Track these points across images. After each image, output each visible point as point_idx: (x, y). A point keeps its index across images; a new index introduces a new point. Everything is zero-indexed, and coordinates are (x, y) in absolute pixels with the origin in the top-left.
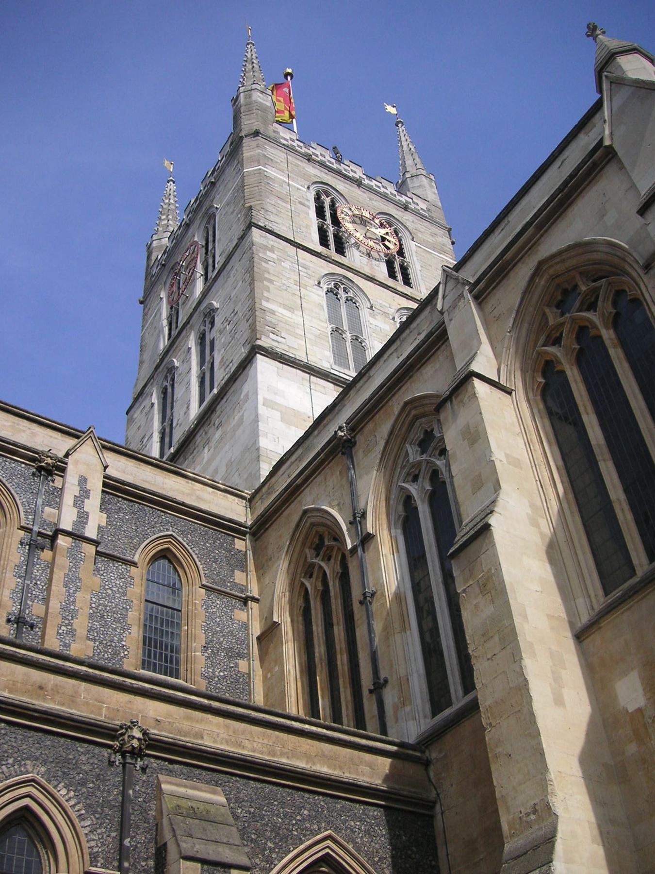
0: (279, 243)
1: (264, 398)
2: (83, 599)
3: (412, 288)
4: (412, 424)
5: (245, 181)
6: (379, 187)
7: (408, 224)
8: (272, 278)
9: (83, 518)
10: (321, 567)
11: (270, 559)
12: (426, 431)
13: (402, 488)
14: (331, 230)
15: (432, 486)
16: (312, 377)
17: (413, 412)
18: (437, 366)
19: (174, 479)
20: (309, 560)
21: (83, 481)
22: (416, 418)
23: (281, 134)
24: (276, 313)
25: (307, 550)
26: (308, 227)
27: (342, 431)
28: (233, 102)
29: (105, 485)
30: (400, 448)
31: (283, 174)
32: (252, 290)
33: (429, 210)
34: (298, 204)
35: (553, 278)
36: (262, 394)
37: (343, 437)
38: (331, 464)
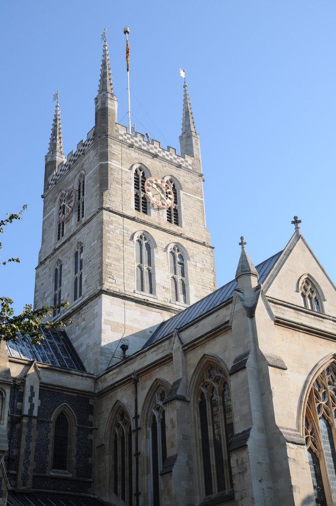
0: (115, 217)
2: (33, 445)
9: (32, 406)
17: (159, 383)
19: (67, 376)
21: (32, 388)
22: (160, 385)
23: (120, 132)
26: (130, 198)
29: (40, 386)
30: (154, 394)
32: (102, 251)
36: (104, 317)
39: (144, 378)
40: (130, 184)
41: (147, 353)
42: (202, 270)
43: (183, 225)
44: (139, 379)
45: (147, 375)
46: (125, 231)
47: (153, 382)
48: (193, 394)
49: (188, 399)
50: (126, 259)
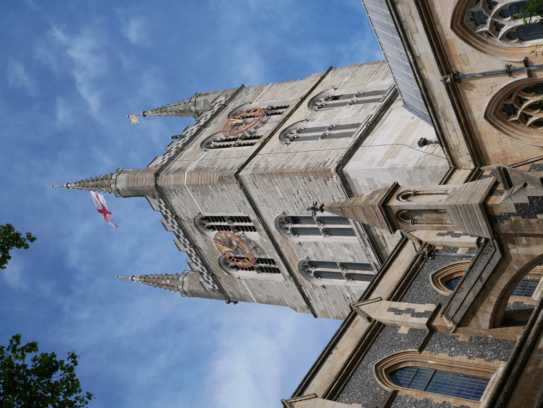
1: (377, 166)
3: (289, 106)
4: (464, 27)
5: (194, 183)
6: (206, 119)
7: (238, 105)
8: (281, 164)
10: (524, 109)
11: (504, 151)
12: (471, 20)
13: (501, 39)
17: (458, 24)
20: (516, 118)
22: (462, 23)
23: (158, 163)
24: (310, 162)
26: (238, 151)
27: (448, 78)
28: (118, 195)
31: (192, 163)
33: (226, 96)
34: (219, 156)
37: (451, 79)
38: (460, 92)
40: (221, 151)
42: (353, 76)
43: (293, 98)
46: (274, 152)
50: (308, 150)
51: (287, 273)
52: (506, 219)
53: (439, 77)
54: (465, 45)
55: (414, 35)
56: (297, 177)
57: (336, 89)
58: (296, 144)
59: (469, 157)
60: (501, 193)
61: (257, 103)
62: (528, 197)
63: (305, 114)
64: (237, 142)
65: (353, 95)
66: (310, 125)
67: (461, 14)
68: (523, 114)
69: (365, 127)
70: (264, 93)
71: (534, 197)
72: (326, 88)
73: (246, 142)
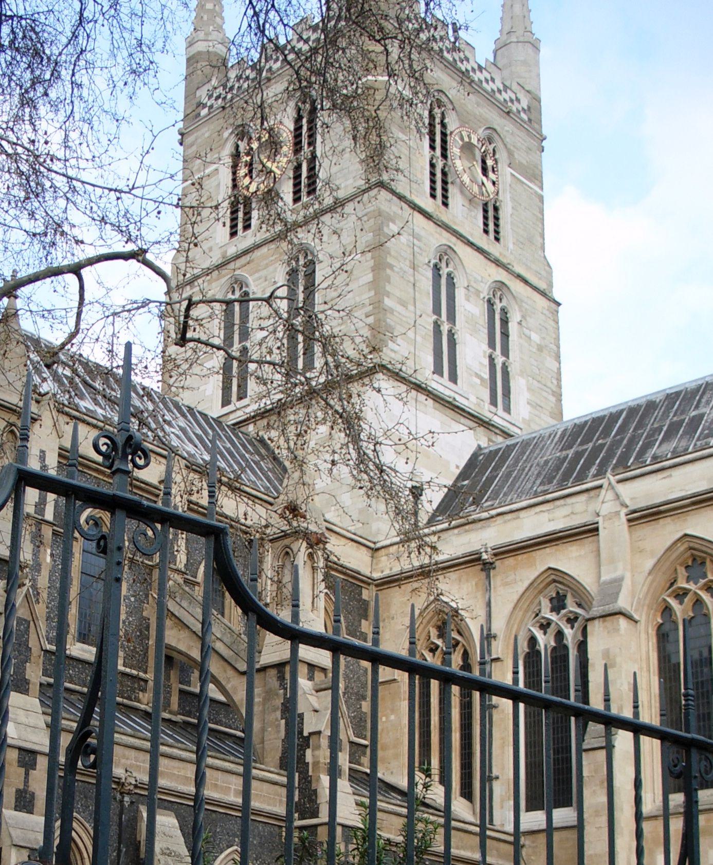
11: (393, 618)
14: (440, 164)
15: (556, 642)
16: (419, 394)
18: (583, 552)
22: (554, 581)
25: (431, 629)
30: (535, 597)
35: (691, 548)
39: (510, 561)
41: (522, 514)
42: (540, 348)
43: (511, 246)
44: (498, 563)
45: (520, 557)
46: (416, 242)
47: (537, 574)
48: (645, 608)
49: (636, 617)
51: (232, 251)
52: (281, 684)
53: (491, 544)
54: (526, 583)
55: (546, 514)
56: (372, 293)
57: (520, 323)
58: (427, 278)
59: (387, 572)
60: (311, 678)
61: (509, 178)
62: (303, 714)
63: (480, 279)
64: (440, 158)
65: (508, 357)
66: (460, 294)
67: (565, 582)
68: (437, 647)
69: (447, 392)
70: (526, 185)
71: (303, 719)
72: (524, 304)
73: (439, 176)
